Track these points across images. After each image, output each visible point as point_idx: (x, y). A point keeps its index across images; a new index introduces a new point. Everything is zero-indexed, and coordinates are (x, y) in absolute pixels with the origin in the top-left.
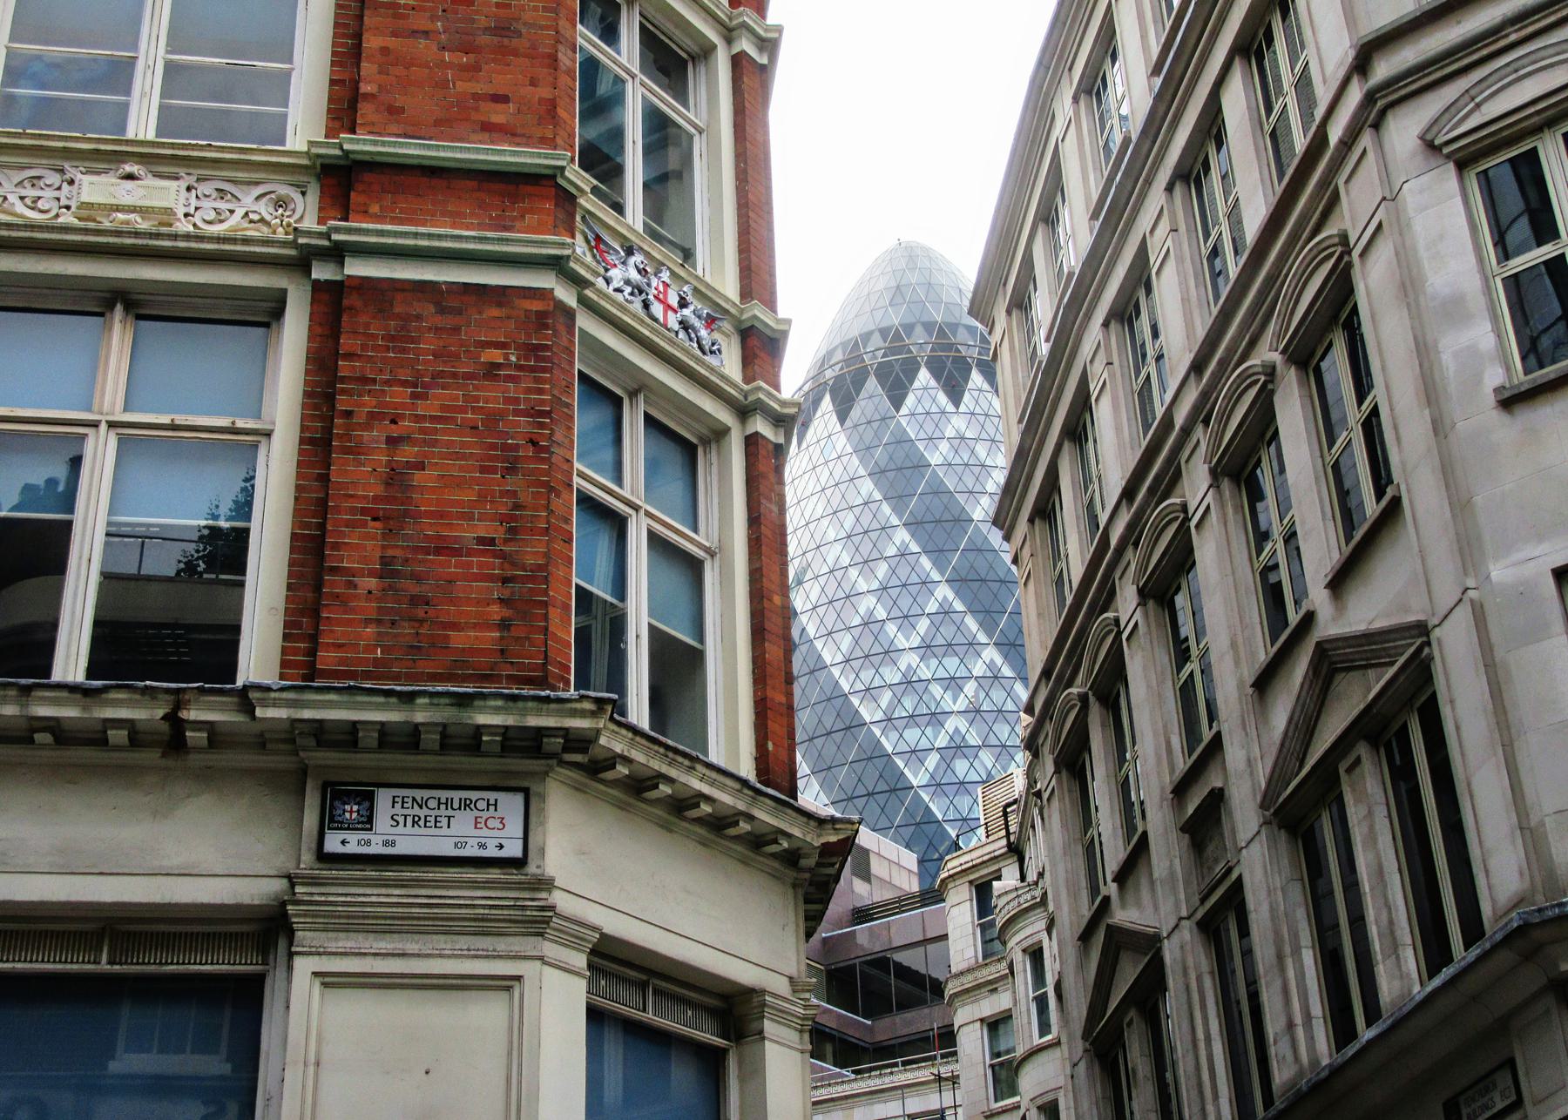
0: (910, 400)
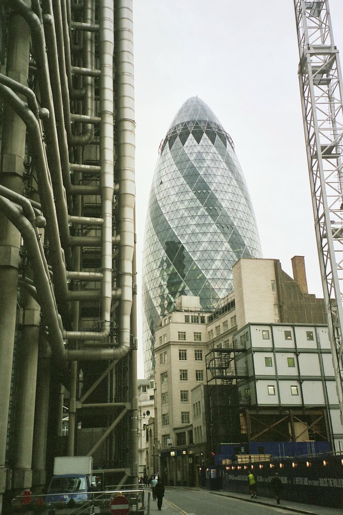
0: (187, 143)
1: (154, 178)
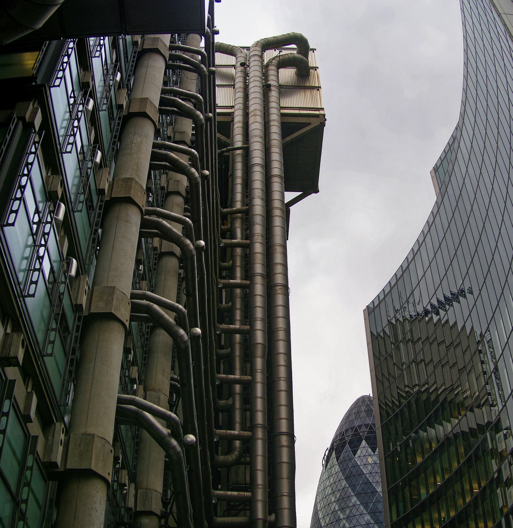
0: (359, 452)
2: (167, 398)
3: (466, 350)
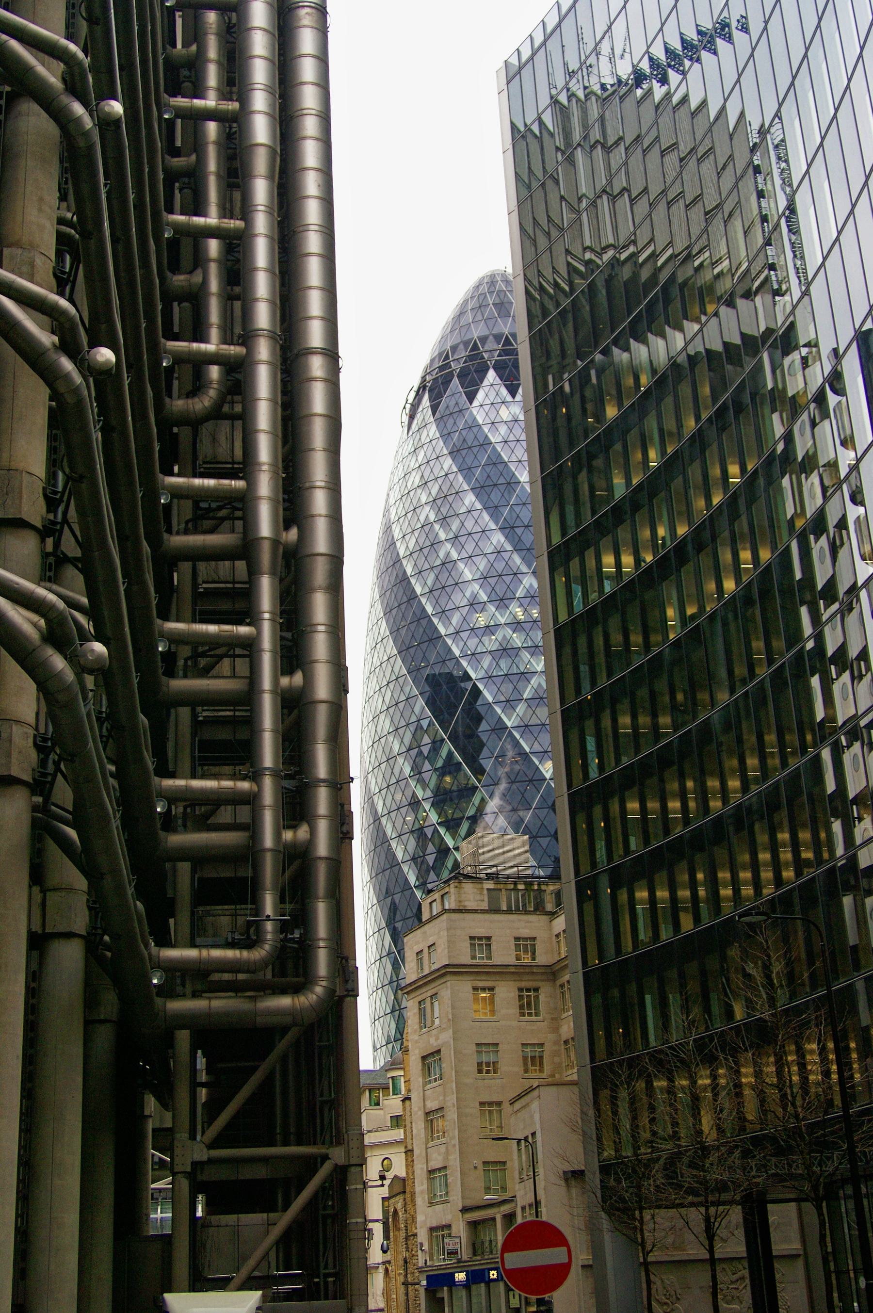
0: (480, 395)
1: (388, 495)
2: (51, 265)
3: (724, 167)
